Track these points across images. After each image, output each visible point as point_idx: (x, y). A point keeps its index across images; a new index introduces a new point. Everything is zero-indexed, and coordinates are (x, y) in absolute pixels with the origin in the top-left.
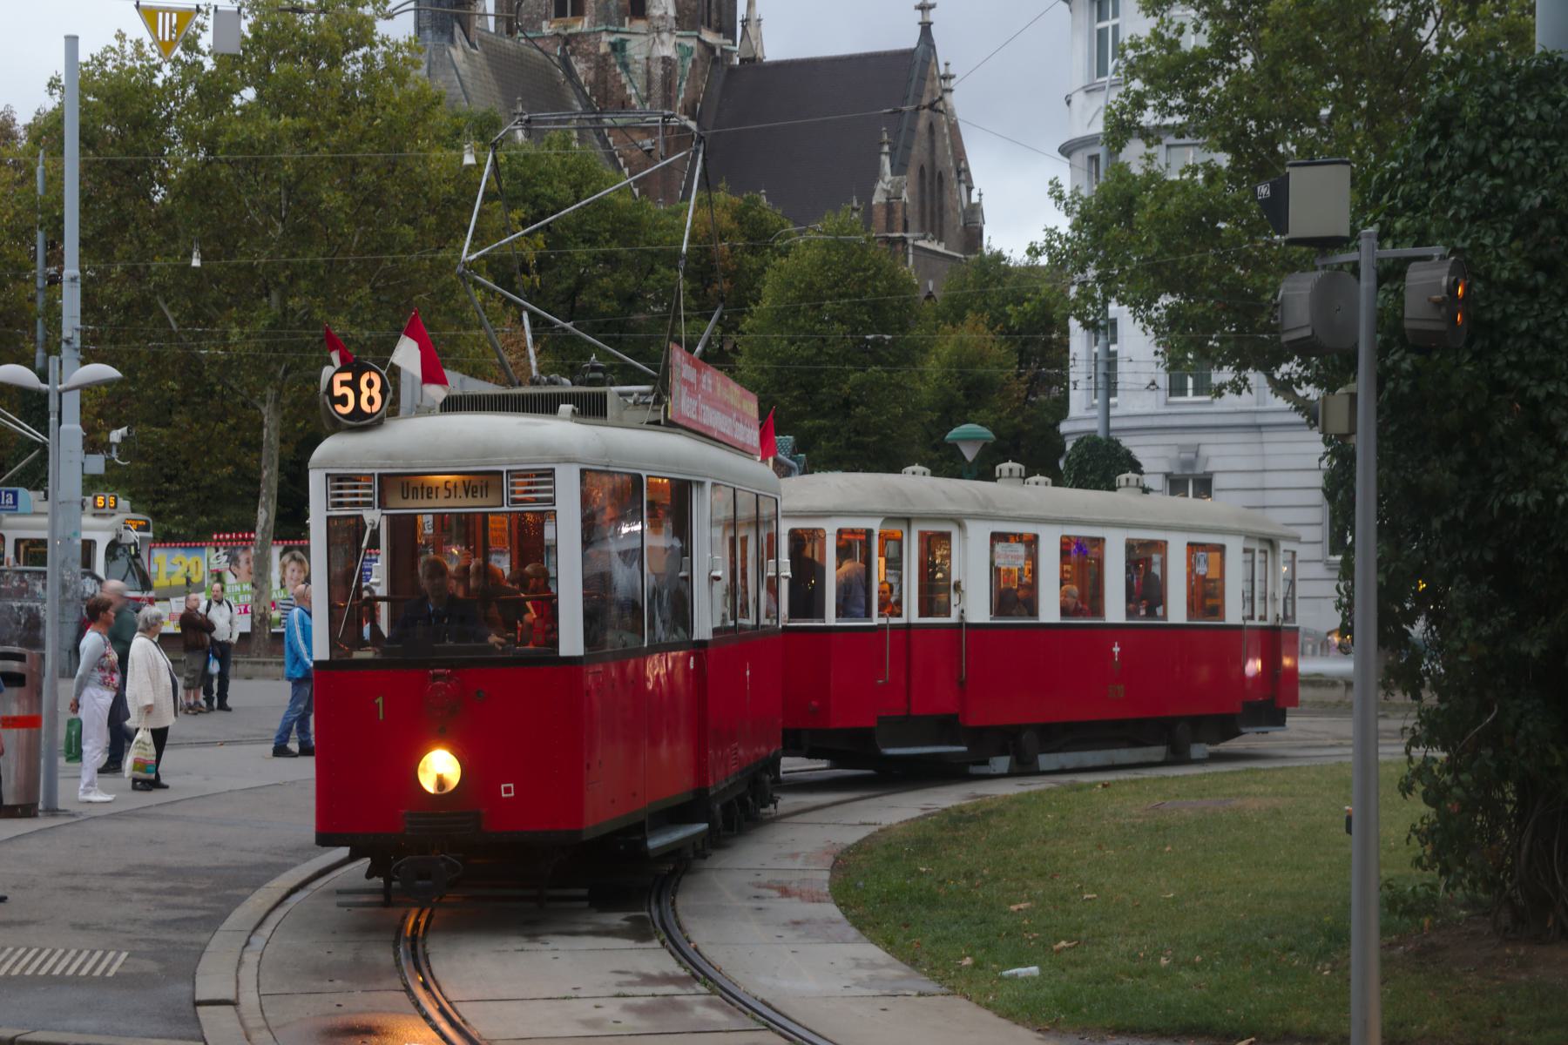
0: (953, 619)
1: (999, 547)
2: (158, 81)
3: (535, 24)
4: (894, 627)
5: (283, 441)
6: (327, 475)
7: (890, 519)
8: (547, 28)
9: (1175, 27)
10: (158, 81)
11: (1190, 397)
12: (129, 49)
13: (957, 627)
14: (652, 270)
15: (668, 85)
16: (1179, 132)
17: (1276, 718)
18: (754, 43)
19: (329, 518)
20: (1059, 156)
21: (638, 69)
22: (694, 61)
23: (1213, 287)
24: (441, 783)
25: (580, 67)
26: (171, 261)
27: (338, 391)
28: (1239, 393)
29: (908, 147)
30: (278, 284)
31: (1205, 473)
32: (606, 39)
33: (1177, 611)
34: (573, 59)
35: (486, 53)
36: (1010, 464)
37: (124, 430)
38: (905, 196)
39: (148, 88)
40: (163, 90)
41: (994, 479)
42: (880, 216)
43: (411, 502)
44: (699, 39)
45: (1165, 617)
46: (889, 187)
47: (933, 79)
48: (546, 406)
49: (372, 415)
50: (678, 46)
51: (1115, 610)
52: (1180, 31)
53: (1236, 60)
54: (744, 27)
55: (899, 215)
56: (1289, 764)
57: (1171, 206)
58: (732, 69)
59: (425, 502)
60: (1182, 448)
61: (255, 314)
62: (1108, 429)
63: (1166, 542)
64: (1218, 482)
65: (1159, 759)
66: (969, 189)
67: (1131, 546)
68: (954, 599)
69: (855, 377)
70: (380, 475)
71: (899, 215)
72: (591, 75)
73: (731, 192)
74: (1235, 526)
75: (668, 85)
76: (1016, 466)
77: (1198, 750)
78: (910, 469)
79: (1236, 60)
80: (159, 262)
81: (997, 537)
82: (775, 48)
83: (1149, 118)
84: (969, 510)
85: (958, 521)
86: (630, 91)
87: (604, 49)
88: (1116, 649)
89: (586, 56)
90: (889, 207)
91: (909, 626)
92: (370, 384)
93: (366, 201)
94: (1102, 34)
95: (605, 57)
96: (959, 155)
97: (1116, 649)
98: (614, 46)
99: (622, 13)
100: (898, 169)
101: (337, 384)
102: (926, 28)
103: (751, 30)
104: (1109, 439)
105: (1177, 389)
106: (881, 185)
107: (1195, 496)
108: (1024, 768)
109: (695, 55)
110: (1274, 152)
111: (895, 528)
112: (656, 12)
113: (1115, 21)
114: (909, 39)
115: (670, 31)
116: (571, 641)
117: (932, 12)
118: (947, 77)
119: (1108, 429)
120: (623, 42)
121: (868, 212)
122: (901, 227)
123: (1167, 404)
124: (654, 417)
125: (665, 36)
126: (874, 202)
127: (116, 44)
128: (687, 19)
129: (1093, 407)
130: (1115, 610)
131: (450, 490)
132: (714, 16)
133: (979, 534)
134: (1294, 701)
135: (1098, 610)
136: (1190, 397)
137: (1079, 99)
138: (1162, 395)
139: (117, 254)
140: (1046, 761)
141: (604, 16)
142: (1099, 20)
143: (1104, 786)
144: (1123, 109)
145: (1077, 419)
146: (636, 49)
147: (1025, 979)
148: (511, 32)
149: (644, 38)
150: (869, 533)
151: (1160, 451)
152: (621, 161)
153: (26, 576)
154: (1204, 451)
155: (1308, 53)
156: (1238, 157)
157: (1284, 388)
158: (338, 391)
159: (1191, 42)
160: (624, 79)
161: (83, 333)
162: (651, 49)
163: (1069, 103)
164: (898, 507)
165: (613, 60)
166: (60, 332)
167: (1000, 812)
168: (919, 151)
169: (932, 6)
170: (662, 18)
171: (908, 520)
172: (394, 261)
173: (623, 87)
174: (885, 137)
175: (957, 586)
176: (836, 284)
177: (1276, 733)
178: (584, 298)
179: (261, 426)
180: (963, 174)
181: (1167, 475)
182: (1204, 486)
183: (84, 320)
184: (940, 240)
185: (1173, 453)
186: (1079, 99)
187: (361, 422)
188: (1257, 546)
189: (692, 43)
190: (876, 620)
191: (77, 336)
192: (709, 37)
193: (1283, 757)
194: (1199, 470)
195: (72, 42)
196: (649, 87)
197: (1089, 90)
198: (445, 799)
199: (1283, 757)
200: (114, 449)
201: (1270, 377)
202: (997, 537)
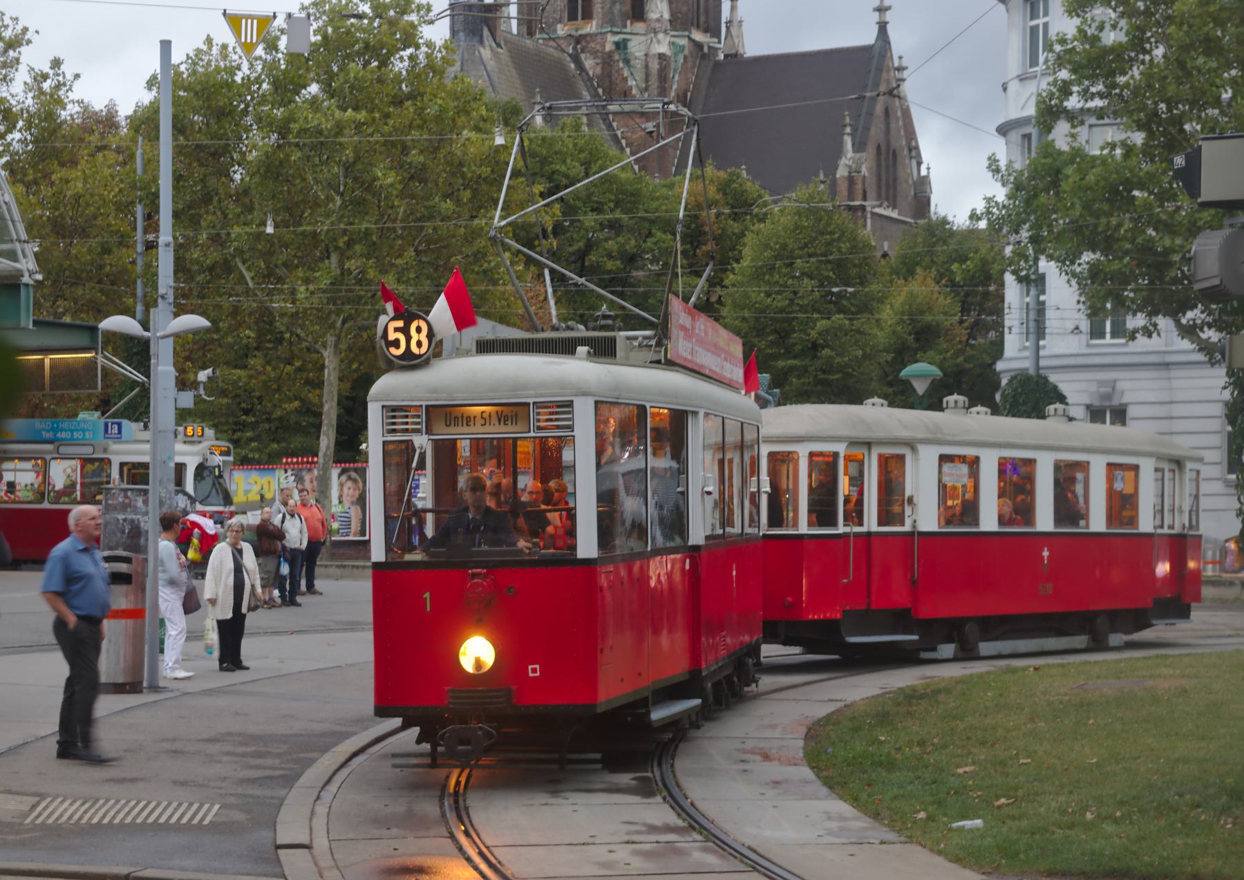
0: (907, 528)
1: (947, 467)
2: (238, 79)
3: (552, 26)
4: (857, 535)
5: (341, 379)
6: (383, 407)
7: (853, 443)
8: (561, 30)
9: (1096, 24)
10: (238, 79)
11: (1108, 339)
12: (215, 51)
13: (912, 534)
14: (650, 234)
15: (663, 77)
16: (1100, 114)
17: (1183, 612)
18: (736, 41)
19: (384, 443)
20: (996, 134)
21: (638, 64)
22: (685, 57)
23: (1128, 246)
24: (478, 664)
25: (589, 63)
26: (248, 230)
27: (392, 336)
28: (1150, 336)
29: (867, 129)
30: (337, 248)
31: (1121, 405)
32: (611, 39)
33: (1097, 522)
34: (583, 56)
35: (510, 51)
36: (955, 397)
37: (209, 371)
38: (864, 171)
39: (230, 85)
40: (243, 85)
41: (941, 409)
42: (843, 187)
43: (452, 429)
44: (690, 38)
45: (1087, 526)
46: (851, 162)
47: (888, 71)
48: (566, 348)
49: (420, 356)
50: (672, 44)
51: (1045, 520)
52: (1101, 28)
53: (1149, 52)
54: (728, 28)
55: (859, 186)
56: (1194, 651)
57: (1091, 178)
58: (717, 64)
59: (465, 429)
60: (1101, 383)
61: (317, 274)
62: (1038, 367)
63: (1088, 463)
64: (1132, 412)
65: (1082, 646)
66: (919, 163)
67: (1058, 467)
68: (908, 511)
69: (822, 324)
70: (427, 407)
71: (859, 186)
72: (598, 70)
73: (719, 168)
74: (1148, 449)
75: (663, 77)
76: (961, 399)
77: (1116, 639)
78: (870, 401)
79: (1149, 52)
80: (236, 230)
81: (944, 459)
82: (753, 46)
83: (1073, 103)
84: (920, 435)
85: (911, 445)
86: (631, 83)
87: (609, 47)
88: (1046, 554)
89: (594, 54)
90: (851, 180)
91: (869, 534)
92: (419, 330)
93: (412, 178)
94: (1034, 30)
95: (610, 54)
96: (911, 135)
97: (1046, 554)
98: (617, 44)
99: (624, 17)
100: (859, 147)
101: (391, 330)
102: (883, 27)
103: (734, 31)
104: (1039, 376)
105: (1097, 332)
106: (844, 162)
107: (1113, 423)
108: (967, 653)
109: (686, 52)
110: (1182, 131)
111: (858, 451)
112: (653, 16)
113: (1045, 20)
114: (866, 36)
115: (665, 32)
116: (587, 546)
117: (888, 13)
118: (900, 69)
119: (1038, 367)
120: (625, 41)
121: (833, 186)
122: (860, 197)
123: (1088, 345)
124: (655, 358)
125: (661, 36)
126: (838, 176)
127: (205, 48)
128: (679, 22)
129: (1025, 348)
130: (1045, 520)
131: (486, 419)
132: (702, 19)
133: (928, 456)
134: (1198, 598)
135: (1029, 519)
136: (1108, 339)
137: (1014, 86)
138: (1084, 338)
139: (203, 223)
140: (985, 648)
141: (609, 20)
142: (1032, 18)
143: (1036, 669)
144: (1051, 97)
145: (1011, 359)
146: (637, 47)
147: (971, 830)
148: (530, 33)
149: (642, 38)
150: (836, 455)
152: (624, 142)
153: (129, 493)
154: (1121, 385)
155: (1211, 47)
156: (1151, 135)
157: (1189, 331)
158: (392, 336)
159: (1110, 38)
160: (626, 73)
161: (176, 289)
162: (649, 48)
163: (1005, 89)
164: (861, 434)
165: (617, 57)
166: (157, 289)
167: (948, 691)
168: (876, 132)
169: (889, 8)
170: (658, 20)
171: (869, 445)
172: (435, 229)
173: (625, 79)
174: (848, 120)
175: (910, 500)
176: (806, 246)
177: (1182, 624)
178: (593, 258)
179: (323, 367)
180: (914, 151)
181: (1088, 407)
182: (1120, 415)
183: (177, 279)
184: (894, 208)
185: (1093, 388)
186: (1014, 86)
187: (411, 362)
188: (1166, 466)
189: (683, 42)
190: (841, 529)
191: (171, 294)
192: (698, 36)
193: (1188, 645)
194: (1115, 402)
195: (166, 46)
196: (647, 80)
197: (1022, 78)
198: (482, 679)
199: (1188, 645)
200: (202, 386)
201: (1178, 322)
202: (944, 459)
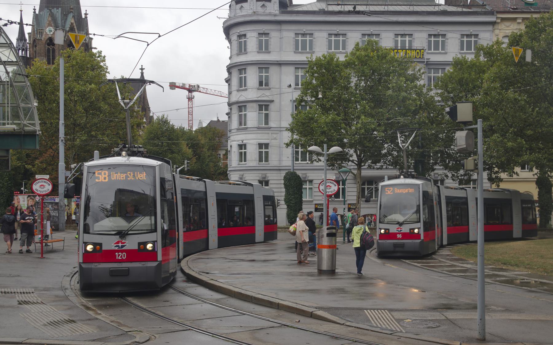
64: (270, 182)
94: (241, 78)
113: (245, 75)
138: (258, 162)
142: (240, 75)
151: (257, 175)
194: (266, 179)
